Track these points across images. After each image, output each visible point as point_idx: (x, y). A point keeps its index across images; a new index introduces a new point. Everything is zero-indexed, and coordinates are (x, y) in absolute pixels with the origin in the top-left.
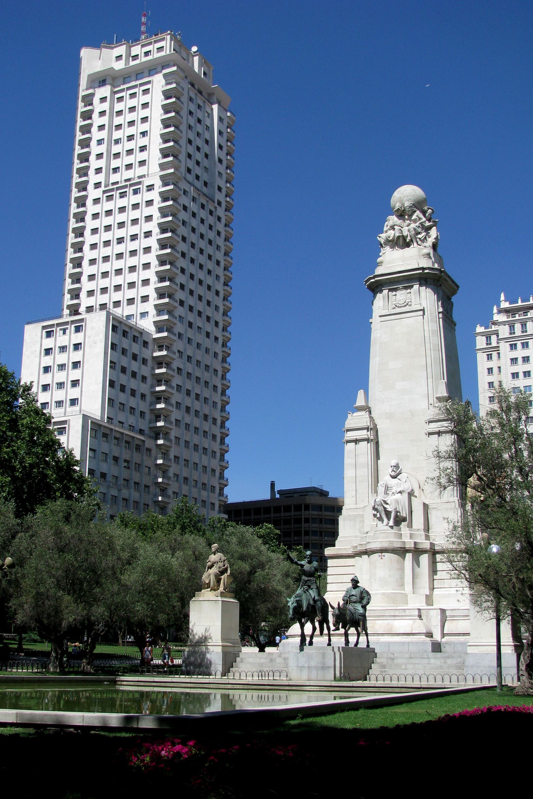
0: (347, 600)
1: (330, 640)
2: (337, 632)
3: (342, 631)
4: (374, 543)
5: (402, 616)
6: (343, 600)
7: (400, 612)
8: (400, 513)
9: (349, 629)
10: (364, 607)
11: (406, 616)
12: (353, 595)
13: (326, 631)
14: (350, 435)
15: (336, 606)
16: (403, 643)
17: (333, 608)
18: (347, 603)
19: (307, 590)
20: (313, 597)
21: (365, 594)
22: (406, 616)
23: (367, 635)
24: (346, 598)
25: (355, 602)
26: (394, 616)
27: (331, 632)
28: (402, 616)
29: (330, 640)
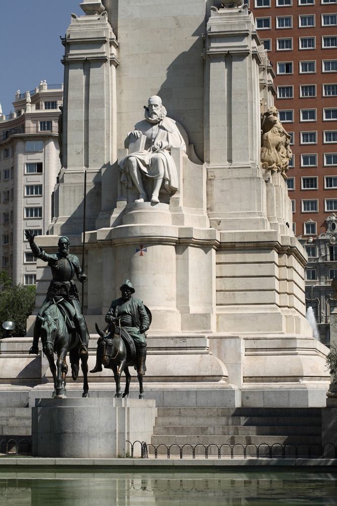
1: (86, 387)
5: (180, 348)
7: (176, 342)
8: (170, 182)
11: (186, 348)
14: (75, 53)
16: (188, 392)
19: (62, 303)
22: (186, 348)
27: (89, 374)
28: (180, 348)
29: (86, 387)
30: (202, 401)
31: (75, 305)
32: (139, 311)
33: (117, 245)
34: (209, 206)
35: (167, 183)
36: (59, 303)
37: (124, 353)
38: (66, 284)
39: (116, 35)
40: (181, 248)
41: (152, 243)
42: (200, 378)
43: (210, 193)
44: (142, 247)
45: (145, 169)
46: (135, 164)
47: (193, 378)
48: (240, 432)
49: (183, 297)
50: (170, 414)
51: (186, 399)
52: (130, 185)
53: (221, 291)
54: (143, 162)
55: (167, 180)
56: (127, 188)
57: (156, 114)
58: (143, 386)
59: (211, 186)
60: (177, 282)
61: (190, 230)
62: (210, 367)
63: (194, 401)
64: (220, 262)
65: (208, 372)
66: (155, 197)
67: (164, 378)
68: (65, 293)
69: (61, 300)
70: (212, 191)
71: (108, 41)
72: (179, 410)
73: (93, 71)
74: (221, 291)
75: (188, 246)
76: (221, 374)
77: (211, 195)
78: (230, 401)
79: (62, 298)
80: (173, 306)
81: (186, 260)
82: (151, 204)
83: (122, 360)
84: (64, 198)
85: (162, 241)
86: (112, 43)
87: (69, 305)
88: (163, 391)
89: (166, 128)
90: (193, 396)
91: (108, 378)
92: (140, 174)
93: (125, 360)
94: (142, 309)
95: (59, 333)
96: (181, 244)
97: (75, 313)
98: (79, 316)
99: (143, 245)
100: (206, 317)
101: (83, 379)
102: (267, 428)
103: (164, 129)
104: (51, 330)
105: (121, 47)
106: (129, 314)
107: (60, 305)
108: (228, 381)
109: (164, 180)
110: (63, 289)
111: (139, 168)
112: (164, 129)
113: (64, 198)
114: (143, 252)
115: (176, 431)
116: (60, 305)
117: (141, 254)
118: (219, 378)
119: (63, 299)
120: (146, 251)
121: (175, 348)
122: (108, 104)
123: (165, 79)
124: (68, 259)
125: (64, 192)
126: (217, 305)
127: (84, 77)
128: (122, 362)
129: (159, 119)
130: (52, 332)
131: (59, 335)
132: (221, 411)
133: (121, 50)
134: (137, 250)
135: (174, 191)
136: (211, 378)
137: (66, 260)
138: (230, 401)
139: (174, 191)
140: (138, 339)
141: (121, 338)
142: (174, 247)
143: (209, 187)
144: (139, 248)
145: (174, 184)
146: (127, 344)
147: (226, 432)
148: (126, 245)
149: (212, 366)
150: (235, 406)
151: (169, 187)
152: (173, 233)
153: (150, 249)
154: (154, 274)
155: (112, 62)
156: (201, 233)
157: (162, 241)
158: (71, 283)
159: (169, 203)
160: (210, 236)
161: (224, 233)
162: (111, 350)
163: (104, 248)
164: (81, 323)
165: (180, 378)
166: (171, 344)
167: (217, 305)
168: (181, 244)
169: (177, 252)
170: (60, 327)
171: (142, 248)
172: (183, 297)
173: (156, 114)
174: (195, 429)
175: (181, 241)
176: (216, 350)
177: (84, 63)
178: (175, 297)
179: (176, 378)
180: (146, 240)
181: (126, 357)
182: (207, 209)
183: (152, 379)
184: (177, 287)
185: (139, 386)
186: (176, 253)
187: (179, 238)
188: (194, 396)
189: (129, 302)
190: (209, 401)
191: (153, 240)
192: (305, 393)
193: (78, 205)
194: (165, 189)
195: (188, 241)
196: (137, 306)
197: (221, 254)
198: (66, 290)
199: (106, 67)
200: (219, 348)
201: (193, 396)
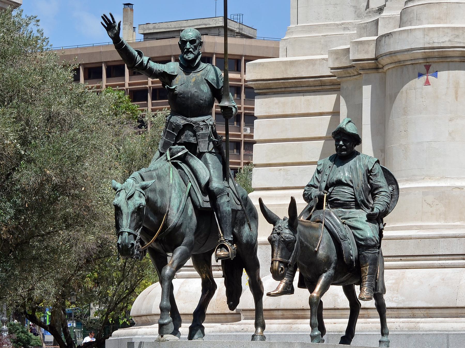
0: (322, 197)
2: (286, 301)
3: (301, 297)
4: (404, 36)
6: (307, 197)
9: (325, 289)
10: (376, 219)
12: (339, 183)
13: (247, 299)
15: (283, 214)
17: (271, 219)
18: (319, 206)
19: (183, 159)
20: (204, 182)
21: (381, 181)
24: (315, 192)
25: (345, 205)
27: (267, 302)
31: (209, 161)
32: (369, 178)
33: (386, 68)
36: (178, 158)
37: (328, 258)
41: (449, 60)
58: (388, 325)
68: (192, 140)
69: (179, 154)
79: (183, 149)
83: (325, 272)
87: (196, 163)
88: (448, 335)
93: (331, 271)
97: (208, 178)
98: (216, 184)
99: (430, 66)
101: (254, 313)
104: (132, 208)
107: (179, 162)
114: (431, 78)
116: (179, 162)
117: (427, 83)
119: (186, 150)
128: (324, 275)
134: (420, 75)
140: (358, 231)
144: (423, 70)
146: (337, 241)
150: (165, 334)
163: (364, 76)
170: (172, 204)
180: (436, 54)
181: (333, 265)
183: (400, 311)
185: (379, 325)
191: (451, 54)
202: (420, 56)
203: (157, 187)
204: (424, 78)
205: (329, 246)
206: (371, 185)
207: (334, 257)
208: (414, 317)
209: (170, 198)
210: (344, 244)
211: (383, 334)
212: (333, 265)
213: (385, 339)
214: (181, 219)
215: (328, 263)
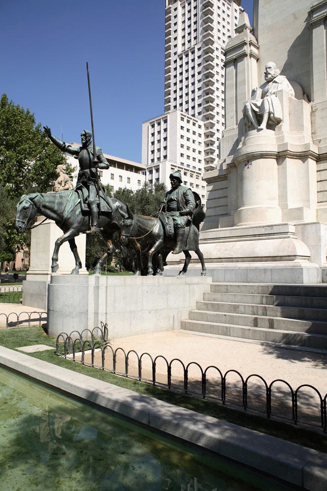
8: (273, 114)
16: (265, 270)
23: (201, 259)
26: (260, 235)
30: (276, 278)
34: (313, 131)
35: (272, 115)
37: (158, 234)
38: (86, 172)
39: (257, 41)
40: (281, 160)
42: (279, 258)
43: (313, 122)
44: (248, 162)
45: (257, 110)
46: (249, 107)
47: (274, 258)
48: (268, 312)
49: (283, 196)
50: (219, 290)
51: (264, 276)
52: (250, 124)
53: (321, 191)
54: (256, 105)
55: (272, 113)
56: (249, 127)
57: (270, 74)
59: (314, 116)
60: (279, 186)
61: (286, 144)
62: (287, 248)
63: (270, 277)
64: (319, 169)
65: (284, 253)
66: (264, 125)
67: (252, 259)
68: (85, 180)
70: (315, 119)
71: (248, 43)
72: (226, 287)
73: (239, 64)
74: (321, 191)
75: (286, 157)
76: (295, 254)
77: (314, 123)
78: (299, 278)
80: (275, 203)
81: (285, 168)
82: (257, 131)
83: (157, 240)
84: (223, 146)
85: (263, 156)
86: (251, 44)
89: (277, 81)
90: (269, 273)
91: (215, 260)
92: (253, 113)
94: (187, 195)
95: (64, 215)
96: (280, 157)
100: (300, 210)
102: (295, 310)
103: (276, 82)
105: (260, 48)
106: (175, 200)
108: (311, 260)
109: (270, 113)
110: (84, 177)
111: (253, 111)
112: (276, 82)
113: (223, 146)
115: (213, 308)
117: (248, 168)
118: (294, 257)
120: (251, 164)
121: (265, 235)
122: (248, 82)
123: (287, 58)
124: (87, 149)
125: (223, 143)
126: (318, 203)
127: (234, 71)
129: (272, 77)
130: (21, 210)
131: (64, 216)
132: (261, 288)
133: (260, 50)
134: (246, 165)
135: (279, 121)
136: (287, 258)
137: (86, 150)
138: (299, 278)
139: (279, 121)
141: (159, 221)
142: (275, 160)
143: (313, 117)
145: (278, 115)
147: (255, 312)
148: (240, 163)
149: (288, 247)
151: (274, 118)
152: (274, 149)
153: (254, 162)
154: (257, 181)
155: (251, 55)
156: (298, 147)
157: (263, 156)
158: (91, 171)
159: (274, 130)
160: (306, 148)
161: (321, 148)
162: (130, 229)
164: (92, 205)
165: (264, 258)
166: (263, 231)
167: (318, 203)
168: (280, 157)
169: (278, 163)
171: (248, 163)
172: (283, 196)
173: (270, 74)
174: (229, 306)
175: (280, 155)
176: (300, 235)
177: (234, 62)
178: (277, 197)
179: (261, 258)
181: (162, 237)
182: (312, 133)
184: (279, 189)
186: (278, 165)
187: (278, 152)
188: (270, 274)
189: (177, 190)
190: (282, 278)
191: (256, 155)
192: (299, 270)
193: (231, 149)
194: (272, 121)
195: (285, 153)
196: (182, 192)
197: (320, 163)
198: (86, 178)
199: (247, 60)
200: (303, 233)
201: (269, 273)
202: (245, 157)
203: (57, 201)
204: (247, 166)
205: (159, 229)
206: (185, 199)
207: (162, 233)
208: (238, 261)
209: (65, 206)
210: (167, 227)
211: (203, 270)
212: (162, 237)
213: (204, 272)
214: (69, 216)
215: (158, 236)
